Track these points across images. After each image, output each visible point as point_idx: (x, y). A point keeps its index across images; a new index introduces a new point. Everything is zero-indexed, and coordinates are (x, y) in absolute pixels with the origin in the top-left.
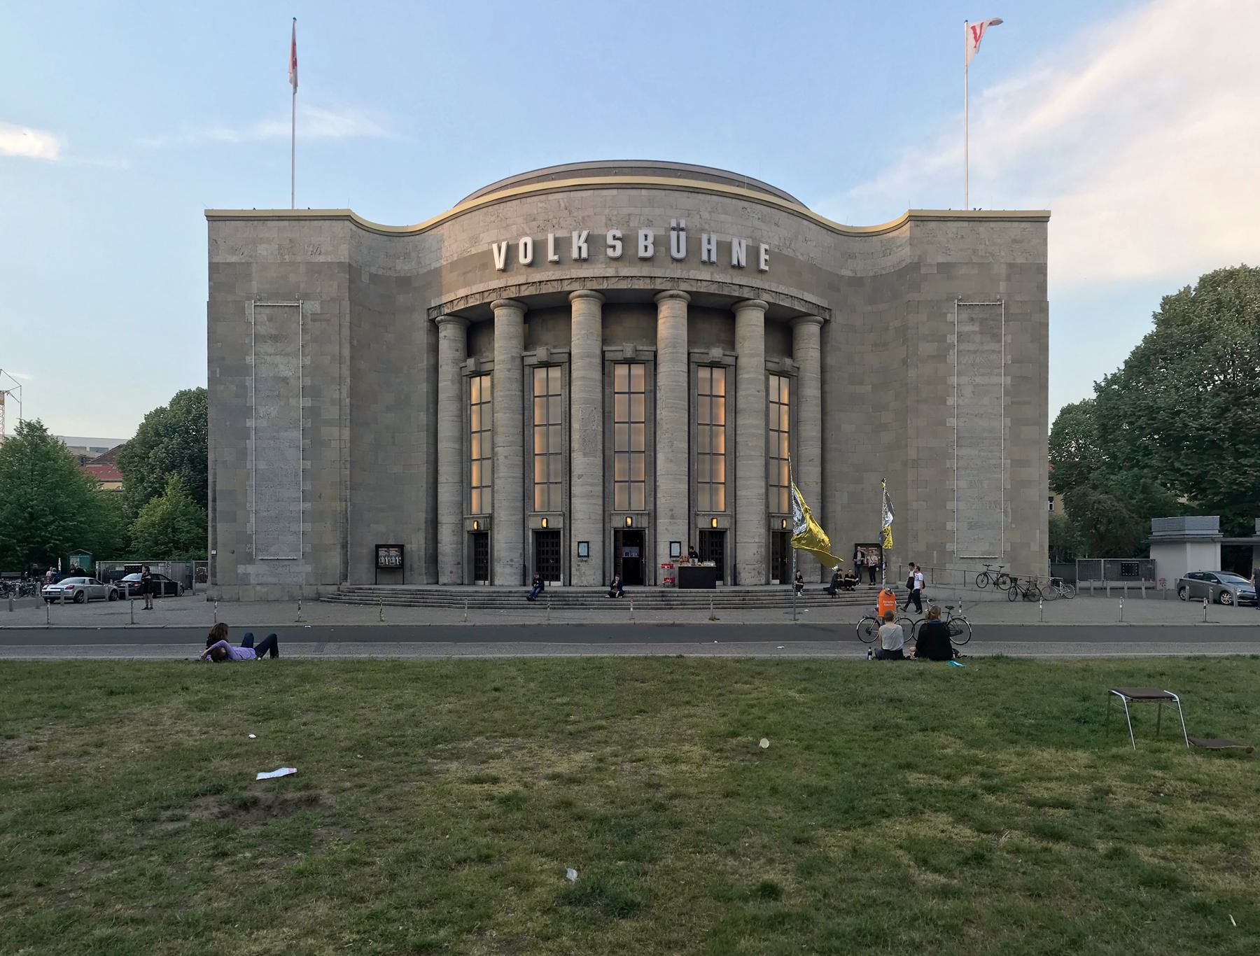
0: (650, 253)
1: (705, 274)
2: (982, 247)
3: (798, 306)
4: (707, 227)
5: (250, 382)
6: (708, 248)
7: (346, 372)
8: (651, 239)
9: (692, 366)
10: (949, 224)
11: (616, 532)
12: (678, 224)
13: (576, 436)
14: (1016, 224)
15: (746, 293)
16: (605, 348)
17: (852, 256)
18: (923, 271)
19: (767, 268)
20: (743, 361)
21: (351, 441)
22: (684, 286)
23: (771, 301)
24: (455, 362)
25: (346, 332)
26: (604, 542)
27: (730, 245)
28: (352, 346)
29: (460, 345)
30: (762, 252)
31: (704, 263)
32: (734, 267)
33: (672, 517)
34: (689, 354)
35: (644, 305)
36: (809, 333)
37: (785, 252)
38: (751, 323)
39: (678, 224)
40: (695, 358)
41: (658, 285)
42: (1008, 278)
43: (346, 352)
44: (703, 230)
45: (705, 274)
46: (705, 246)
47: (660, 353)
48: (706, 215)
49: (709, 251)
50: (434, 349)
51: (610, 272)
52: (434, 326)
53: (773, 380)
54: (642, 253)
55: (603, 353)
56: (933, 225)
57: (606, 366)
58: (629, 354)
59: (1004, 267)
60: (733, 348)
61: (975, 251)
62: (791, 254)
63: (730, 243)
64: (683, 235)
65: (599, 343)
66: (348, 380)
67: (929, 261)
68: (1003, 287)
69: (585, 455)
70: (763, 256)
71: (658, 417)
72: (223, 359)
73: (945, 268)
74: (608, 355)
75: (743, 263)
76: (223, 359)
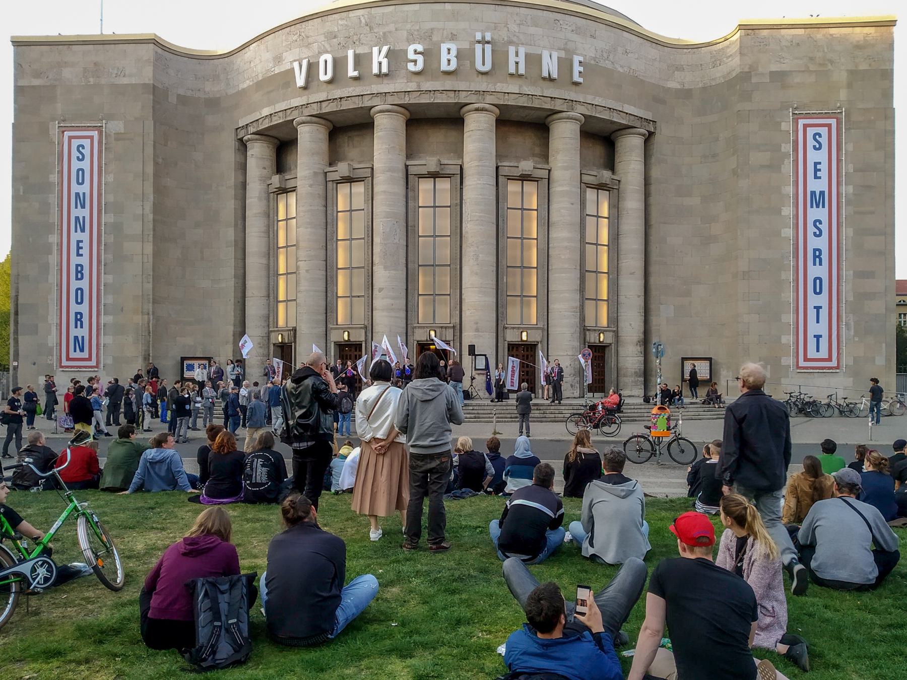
0: (453, 66)
1: (513, 87)
3: (616, 118)
4: (515, 39)
5: (53, 199)
6: (516, 59)
8: (454, 53)
9: (500, 178)
12: (483, 37)
13: (377, 249)
16: (408, 163)
17: (680, 68)
18: (754, 80)
19: (581, 80)
20: (557, 174)
22: (490, 99)
24: (263, 179)
25: (150, 151)
27: (539, 58)
28: (156, 164)
29: (268, 163)
31: (512, 75)
32: (544, 79)
33: (477, 330)
34: (497, 168)
35: (451, 119)
36: (630, 149)
37: (602, 64)
38: (565, 137)
39: (483, 37)
40: (502, 171)
43: (150, 169)
44: (511, 43)
45: (513, 87)
46: (512, 59)
47: (465, 166)
48: (514, 27)
49: (517, 63)
50: (243, 167)
51: (412, 86)
52: (242, 145)
53: (591, 194)
54: (444, 67)
55: (407, 166)
56: (765, 33)
57: (409, 180)
58: (433, 168)
62: (610, 66)
63: (541, 55)
64: (488, 48)
66: (151, 197)
67: (760, 70)
69: (386, 268)
70: (577, 68)
73: (779, 77)
74: (412, 170)
75: (555, 75)
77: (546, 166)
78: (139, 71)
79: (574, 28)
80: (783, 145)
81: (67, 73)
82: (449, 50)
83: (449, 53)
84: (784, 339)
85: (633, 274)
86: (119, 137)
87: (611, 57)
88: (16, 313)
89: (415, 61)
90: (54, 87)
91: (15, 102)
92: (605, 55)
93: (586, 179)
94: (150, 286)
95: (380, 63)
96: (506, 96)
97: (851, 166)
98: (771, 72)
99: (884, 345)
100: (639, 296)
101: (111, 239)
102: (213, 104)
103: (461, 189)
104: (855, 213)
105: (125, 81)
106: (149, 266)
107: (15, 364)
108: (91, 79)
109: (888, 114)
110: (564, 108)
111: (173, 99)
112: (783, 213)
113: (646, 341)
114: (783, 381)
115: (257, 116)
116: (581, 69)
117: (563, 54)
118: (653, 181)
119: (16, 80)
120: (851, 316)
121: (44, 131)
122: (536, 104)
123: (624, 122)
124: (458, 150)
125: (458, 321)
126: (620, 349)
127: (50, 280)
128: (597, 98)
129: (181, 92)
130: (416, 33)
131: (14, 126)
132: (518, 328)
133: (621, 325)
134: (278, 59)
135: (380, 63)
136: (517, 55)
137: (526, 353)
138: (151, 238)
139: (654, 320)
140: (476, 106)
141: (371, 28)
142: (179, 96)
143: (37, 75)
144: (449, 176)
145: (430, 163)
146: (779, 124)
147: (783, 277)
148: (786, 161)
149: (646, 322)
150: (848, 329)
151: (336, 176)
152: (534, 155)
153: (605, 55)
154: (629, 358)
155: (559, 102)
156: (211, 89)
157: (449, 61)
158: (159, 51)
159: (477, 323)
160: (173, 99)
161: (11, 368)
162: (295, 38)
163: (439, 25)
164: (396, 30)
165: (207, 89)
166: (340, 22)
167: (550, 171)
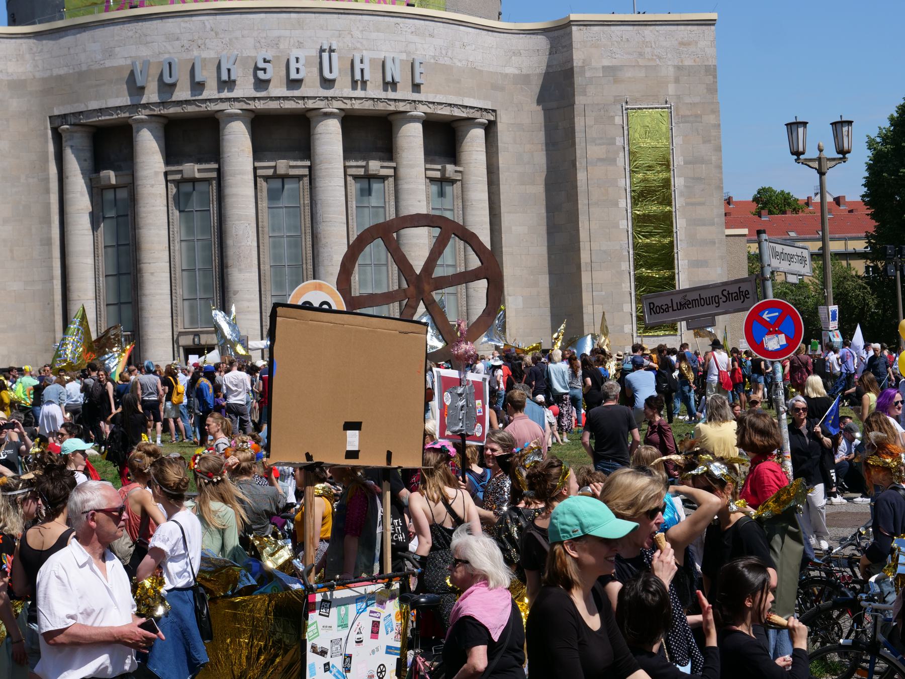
2: (648, 50)
3: (457, 113)
4: (359, 45)
9: (349, 179)
10: (613, 28)
14: (683, 27)
15: (401, 107)
16: (257, 164)
18: (588, 74)
20: (402, 172)
23: (429, 111)
30: (417, 65)
34: (345, 167)
36: (474, 142)
37: (441, 61)
41: (310, 104)
42: (677, 80)
49: (362, 70)
54: (294, 75)
55: (255, 169)
59: (671, 71)
61: (641, 54)
62: (447, 62)
65: (251, 159)
67: (594, 64)
68: (671, 89)
73: (611, 71)
74: (259, 172)
75: (397, 79)
77: (394, 164)
79: (413, 29)
82: (297, 60)
83: (297, 62)
87: (449, 54)
89: (264, 70)
92: (444, 52)
95: (229, 70)
97: (681, 159)
98: (603, 67)
104: (687, 204)
112: (620, 206)
115: (82, 108)
116: (422, 70)
117: (404, 57)
122: (381, 106)
123: (464, 115)
128: (438, 96)
130: (263, 40)
134: (109, 53)
135: (229, 70)
136: (362, 62)
141: (217, 33)
146: (613, 117)
151: (178, 177)
153: (444, 52)
155: (402, 104)
157: (298, 70)
162: (130, 34)
164: (243, 36)
165: (10, 70)
166: (183, 25)
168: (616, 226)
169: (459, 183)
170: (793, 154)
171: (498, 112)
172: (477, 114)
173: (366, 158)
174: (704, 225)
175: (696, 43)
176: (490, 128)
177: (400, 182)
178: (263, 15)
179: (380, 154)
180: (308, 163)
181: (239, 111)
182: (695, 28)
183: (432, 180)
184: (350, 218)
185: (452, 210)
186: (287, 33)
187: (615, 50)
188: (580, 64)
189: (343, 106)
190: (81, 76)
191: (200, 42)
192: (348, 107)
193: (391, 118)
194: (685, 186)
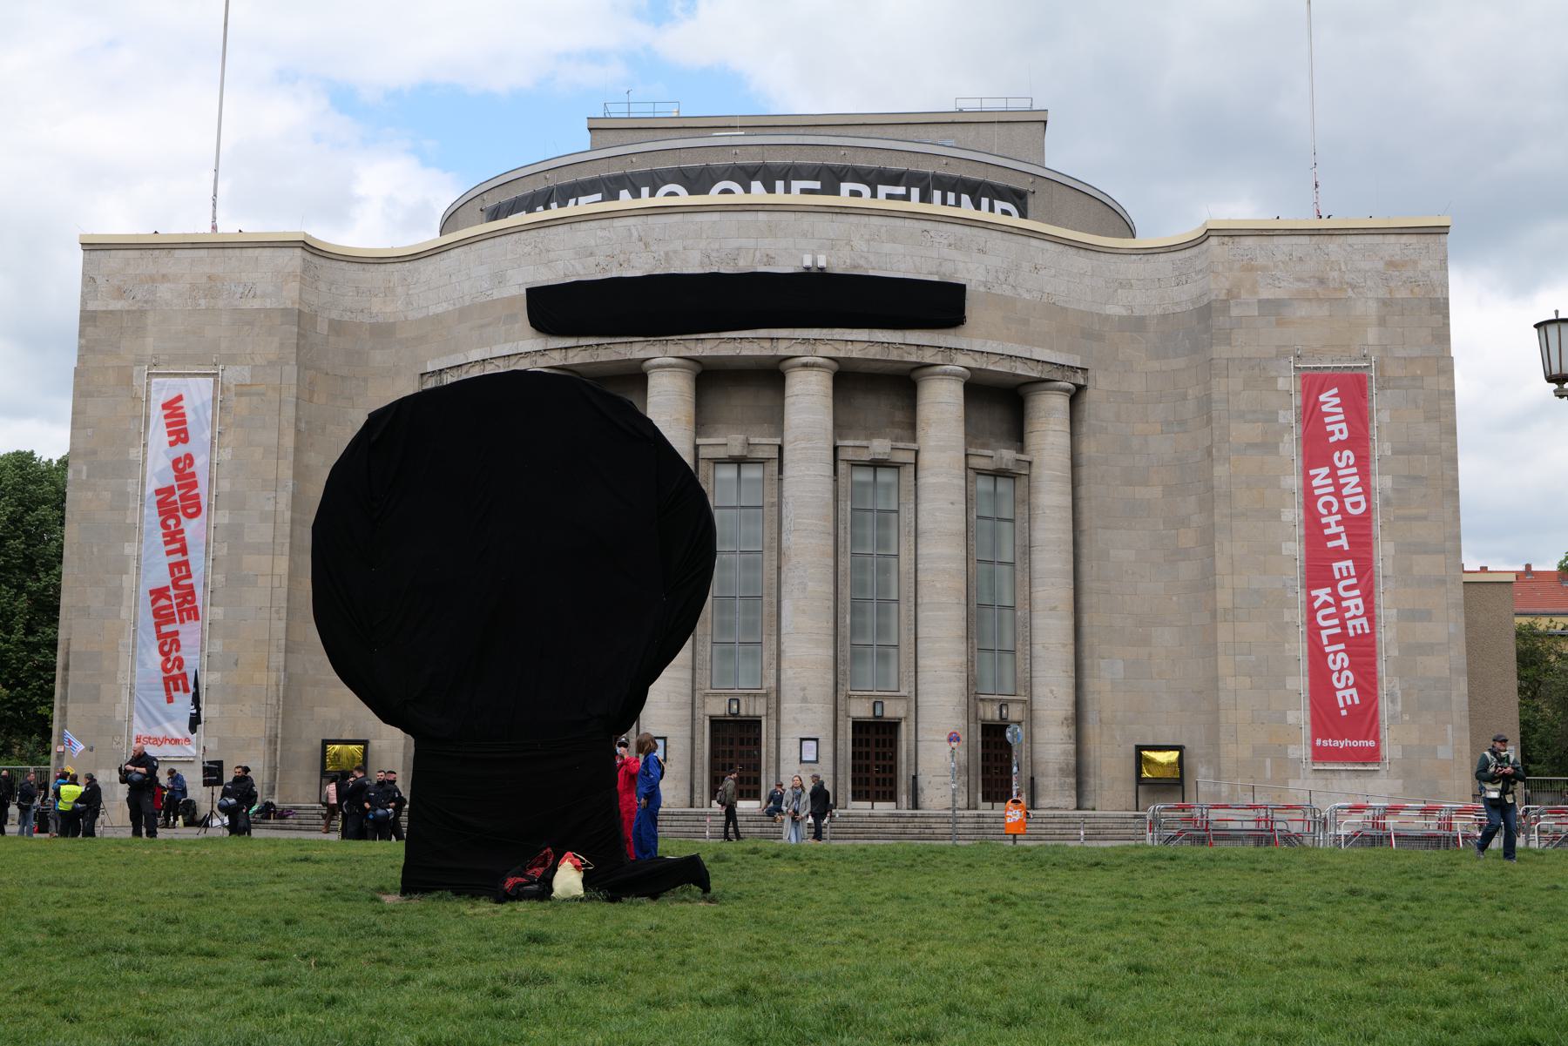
2: (1336, 274)
3: (1021, 370)
4: (862, 262)
7: (287, 472)
9: (842, 466)
11: (715, 723)
14: (1392, 239)
16: (699, 441)
18: (1235, 312)
20: (925, 459)
21: (290, 580)
23: (973, 365)
25: (289, 412)
26: (693, 739)
28: (298, 431)
33: (804, 700)
34: (836, 449)
37: (997, 290)
38: (942, 404)
40: (842, 455)
42: (1382, 322)
43: (289, 441)
48: (861, 245)
56: (1249, 241)
58: (736, 450)
59: (1373, 307)
60: (914, 440)
61: (1322, 281)
62: (1007, 291)
67: (1244, 296)
71: (784, 544)
72: (94, 453)
73: (1272, 308)
74: (703, 453)
76: (94, 453)
77: (912, 446)
78: (273, 284)
80: (1281, 413)
81: (164, 291)
84: (1291, 717)
85: (1054, 609)
86: (242, 390)
87: (1011, 280)
88: (66, 668)
90: (143, 312)
91: (81, 334)
92: (1002, 277)
93: (976, 462)
94: (283, 624)
96: (850, 346)
99: (1450, 727)
100: (1064, 645)
101: (225, 551)
102: (383, 332)
103: (780, 480)
105: (256, 304)
106: (282, 593)
107: (60, 749)
108: (203, 302)
109: (1445, 367)
110: (938, 359)
111: (323, 327)
112: (1284, 518)
113: (1078, 718)
114: (1291, 782)
118: (1084, 459)
119: (84, 301)
120: (1396, 680)
121: (126, 380)
122: (894, 355)
123: (1034, 374)
124: (777, 420)
125: (773, 683)
126: (1036, 730)
127: (124, 614)
129: (335, 315)
131: (77, 372)
132: (869, 697)
133: (1038, 691)
134: (499, 278)
137: (881, 737)
138: (287, 549)
139: (1091, 684)
140: (804, 360)
141: (646, 245)
142: (331, 322)
143: (121, 293)
144: (761, 462)
145: (734, 443)
147: (1287, 618)
148: (1286, 437)
149: (1078, 687)
150: (1393, 701)
152: (893, 424)
153: (1002, 277)
154: (1050, 745)
156: (383, 309)
158: (308, 256)
159: (804, 689)
160: (323, 327)
161: (53, 755)
162: (528, 249)
163: (751, 243)
165: (374, 310)
166: (599, 233)
167: (917, 452)
168: (1277, 550)
169: (1025, 479)
170: (1550, 379)
171: (1090, 373)
172: (1056, 375)
173: (870, 437)
174: (1426, 553)
175: (1415, 262)
176: (1076, 395)
177: (920, 474)
178: (715, 216)
179: (898, 431)
180: (778, 441)
181: (674, 361)
182: (1413, 239)
183: (980, 472)
184: (841, 527)
185: (1012, 521)
186: (751, 243)
187: (1279, 274)
188: (1223, 296)
189: (833, 354)
190: (463, 313)
191: (622, 258)
192: (842, 355)
193: (914, 375)
194: (1395, 490)
